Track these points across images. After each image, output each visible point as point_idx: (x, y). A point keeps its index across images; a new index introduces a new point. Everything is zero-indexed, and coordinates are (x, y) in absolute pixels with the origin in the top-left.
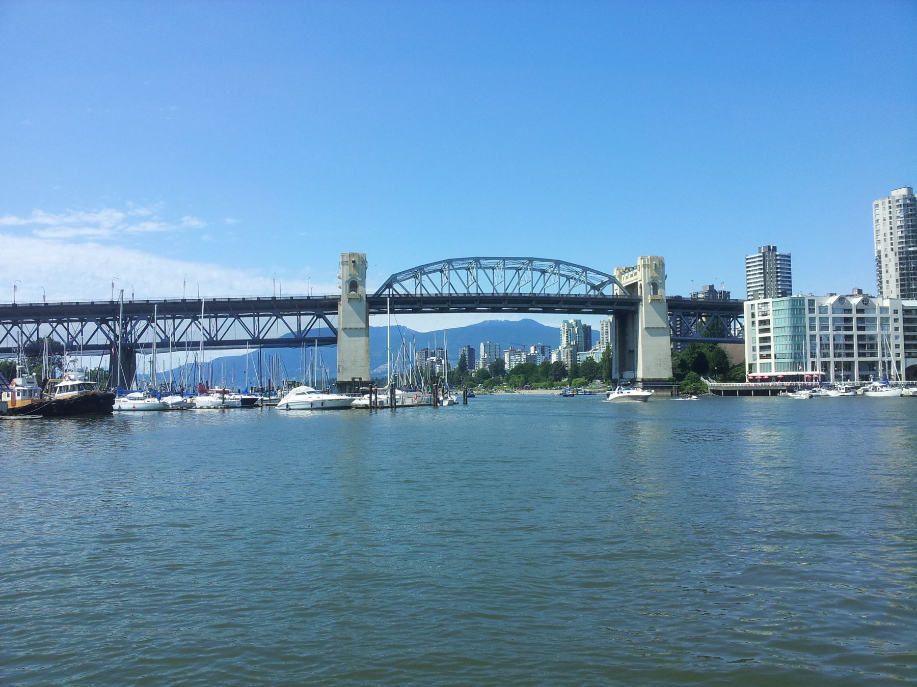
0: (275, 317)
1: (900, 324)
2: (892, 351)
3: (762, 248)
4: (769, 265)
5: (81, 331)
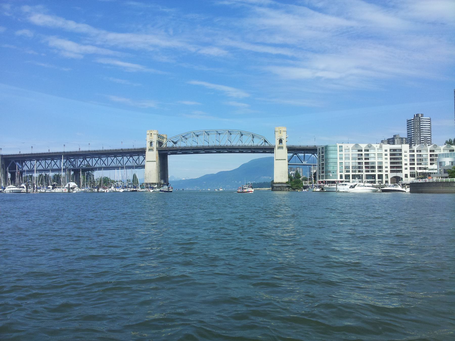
1: (389, 157)
2: (384, 169)
3: (420, 115)
4: (417, 124)
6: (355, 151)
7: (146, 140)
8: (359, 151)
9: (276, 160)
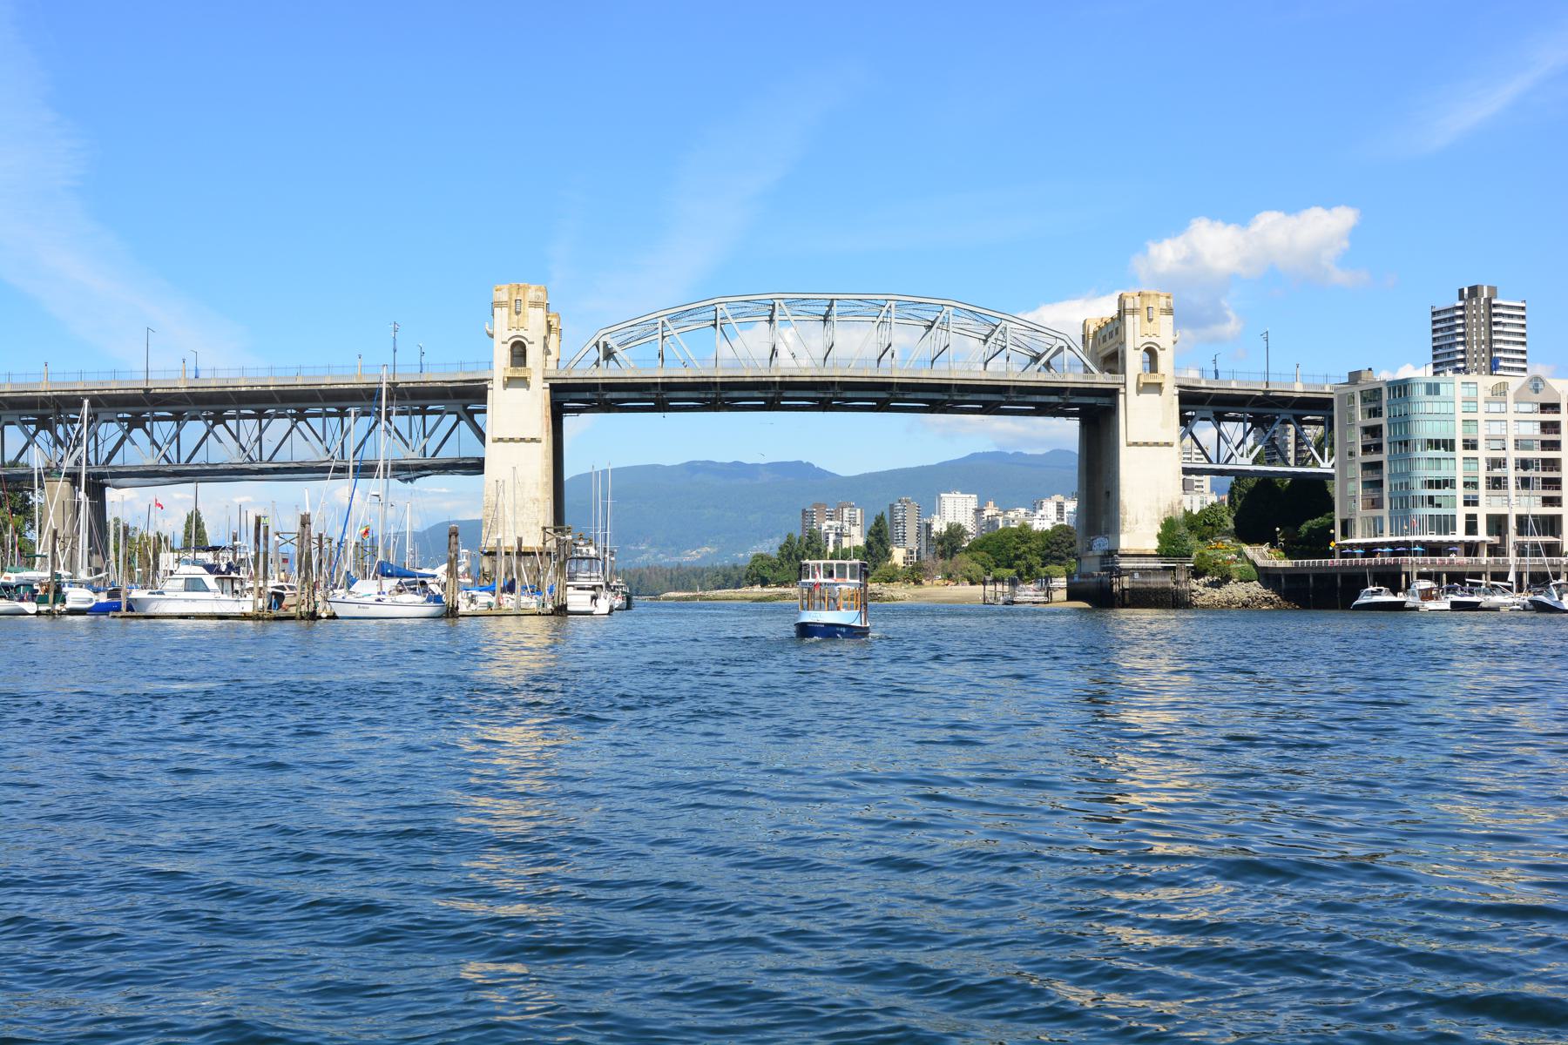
0: (454, 418)
5: (259, 439)
6: (1528, 407)
7: (492, 336)
8: (1545, 408)
9: (1128, 445)
